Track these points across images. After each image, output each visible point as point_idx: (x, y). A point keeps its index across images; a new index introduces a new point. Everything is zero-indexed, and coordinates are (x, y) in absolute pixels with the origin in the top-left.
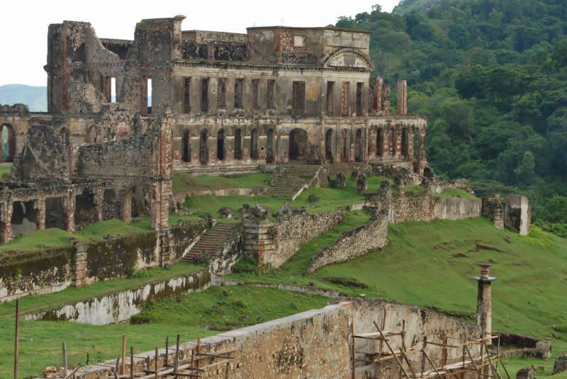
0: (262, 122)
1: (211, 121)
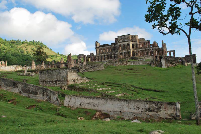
0: (112, 53)
1: (102, 54)
